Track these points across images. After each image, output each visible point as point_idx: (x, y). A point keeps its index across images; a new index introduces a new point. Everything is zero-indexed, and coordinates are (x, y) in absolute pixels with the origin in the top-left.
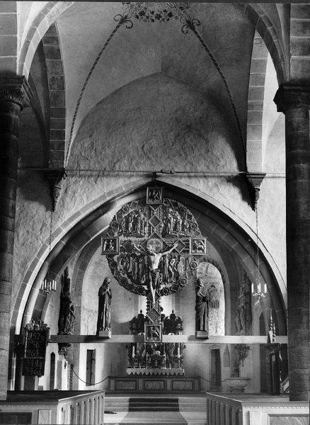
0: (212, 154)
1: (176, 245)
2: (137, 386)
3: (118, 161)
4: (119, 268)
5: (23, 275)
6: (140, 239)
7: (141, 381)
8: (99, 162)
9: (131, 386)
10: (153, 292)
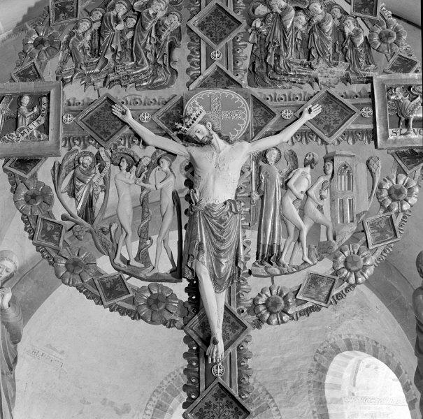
4: (58, 211)
10: (215, 302)
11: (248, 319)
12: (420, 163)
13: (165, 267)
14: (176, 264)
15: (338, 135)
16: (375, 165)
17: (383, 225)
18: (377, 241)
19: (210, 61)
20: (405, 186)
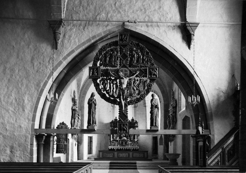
0: (163, 9)
1: (138, 73)
2: (114, 155)
3: (98, 14)
4: (100, 87)
5: (38, 91)
6: (114, 68)
7: (116, 153)
8: (85, 15)
9: (111, 155)
10: (123, 102)
11: (127, 104)
13: (116, 96)
19: (123, 63)
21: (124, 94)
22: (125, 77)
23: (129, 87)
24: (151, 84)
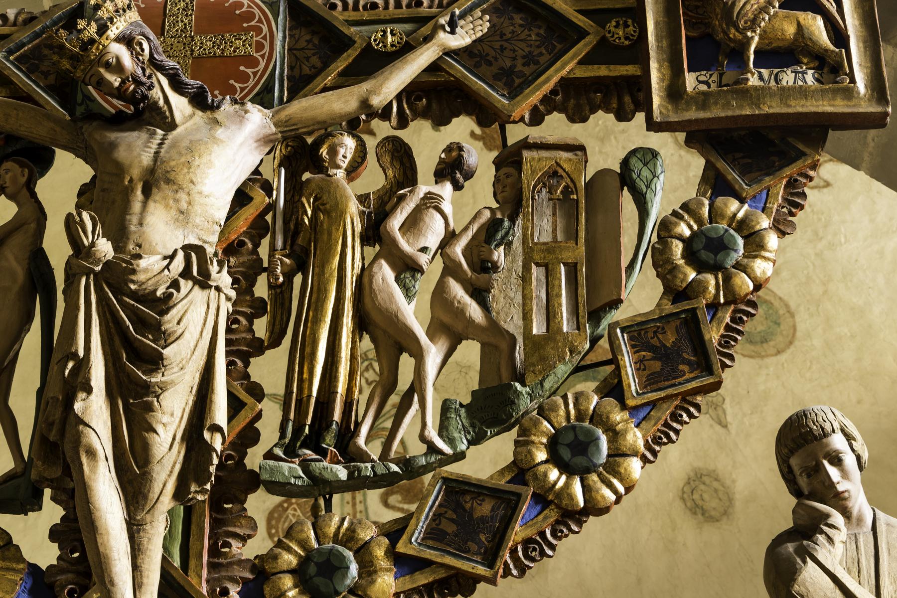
12: (781, 168)
14: (26, 458)
15: (535, 97)
16: (646, 173)
17: (670, 338)
18: (650, 381)
20: (738, 230)
21: (155, 362)
22: (199, 101)
23: (281, 292)
24: (743, 226)
